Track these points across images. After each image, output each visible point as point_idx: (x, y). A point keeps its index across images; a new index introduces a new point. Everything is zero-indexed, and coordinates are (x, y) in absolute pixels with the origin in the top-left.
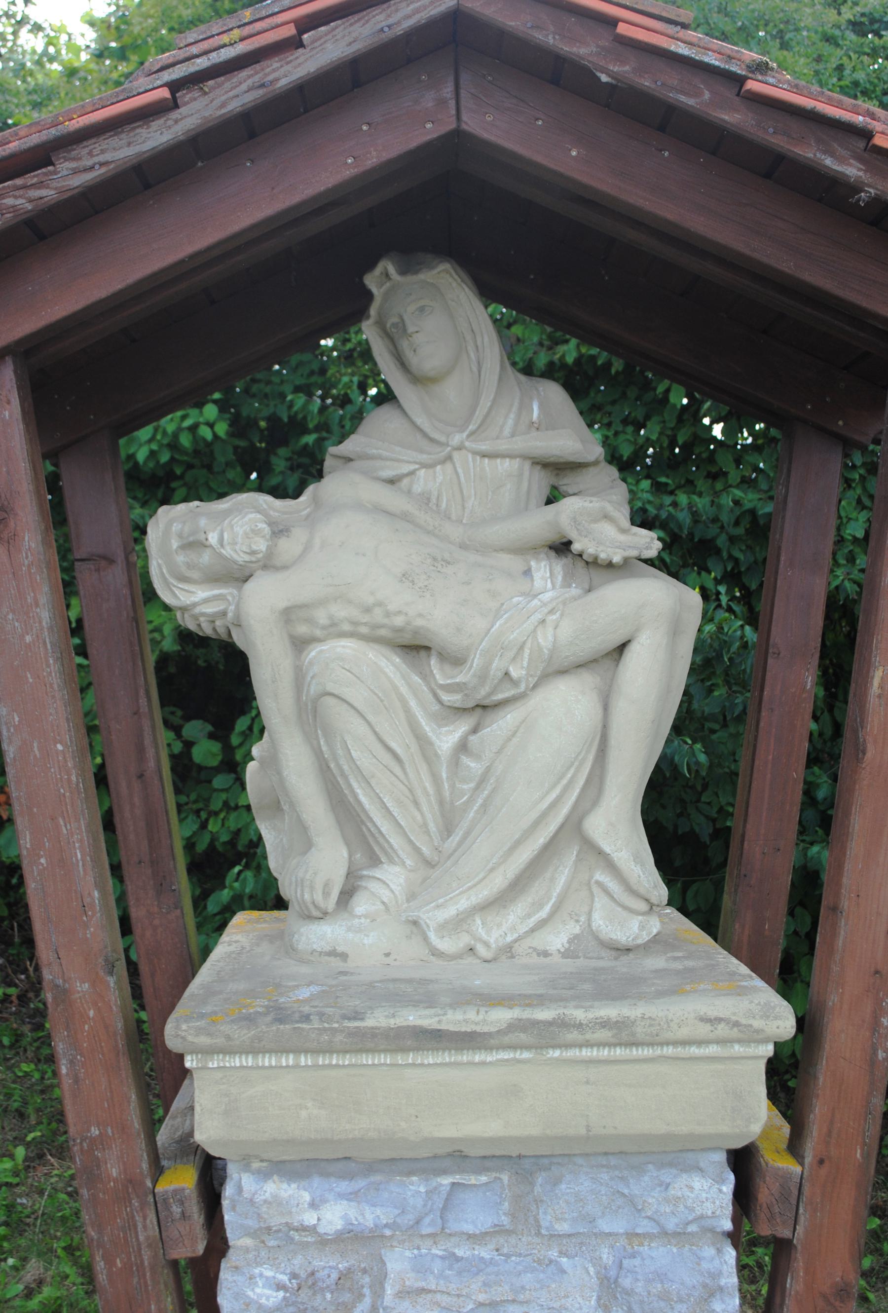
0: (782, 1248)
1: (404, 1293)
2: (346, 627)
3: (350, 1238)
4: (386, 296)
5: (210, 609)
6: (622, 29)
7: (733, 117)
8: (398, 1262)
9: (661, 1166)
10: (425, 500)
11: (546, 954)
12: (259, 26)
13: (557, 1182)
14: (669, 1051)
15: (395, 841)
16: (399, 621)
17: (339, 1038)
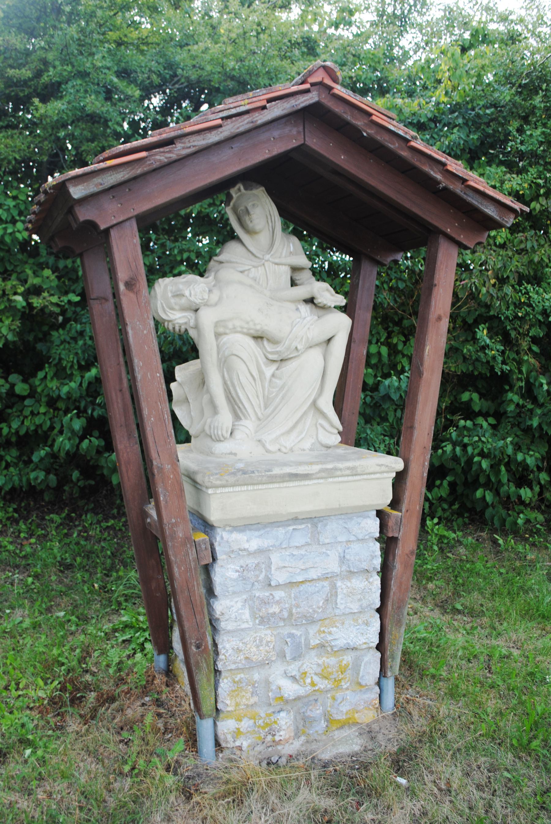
0: (394, 540)
1: (278, 569)
2: (239, 329)
3: (260, 551)
4: (238, 198)
5: (181, 321)
6: (374, 118)
7: (405, 153)
8: (275, 558)
9: (358, 517)
10: (255, 279)
11: (304, 450)
12: (254, 99)
13: (326, 525)
14: (365, 477)
15: (250, 411)
16: (258, 327)
17: (265, 478)
